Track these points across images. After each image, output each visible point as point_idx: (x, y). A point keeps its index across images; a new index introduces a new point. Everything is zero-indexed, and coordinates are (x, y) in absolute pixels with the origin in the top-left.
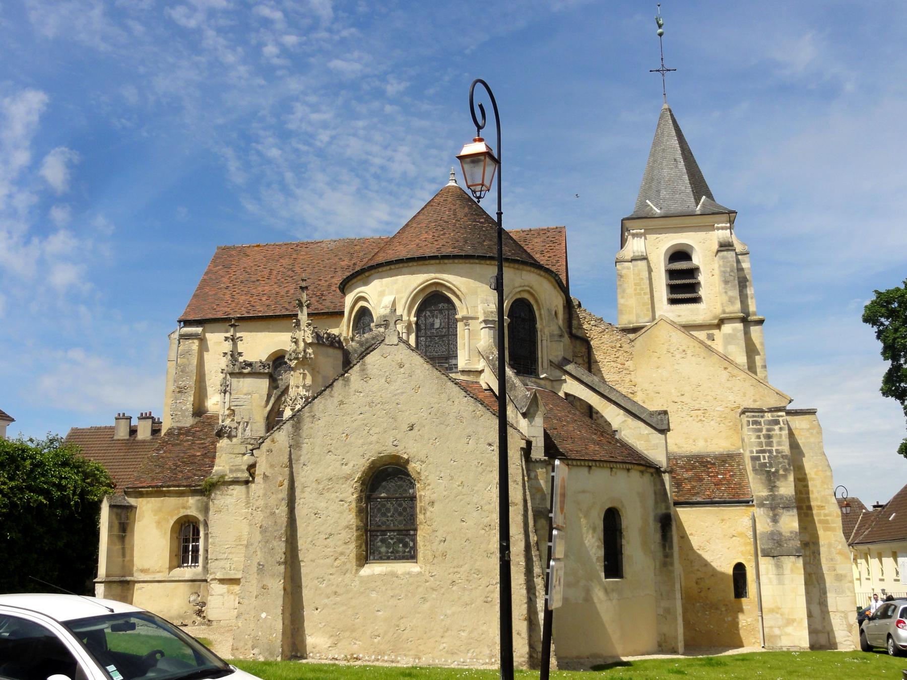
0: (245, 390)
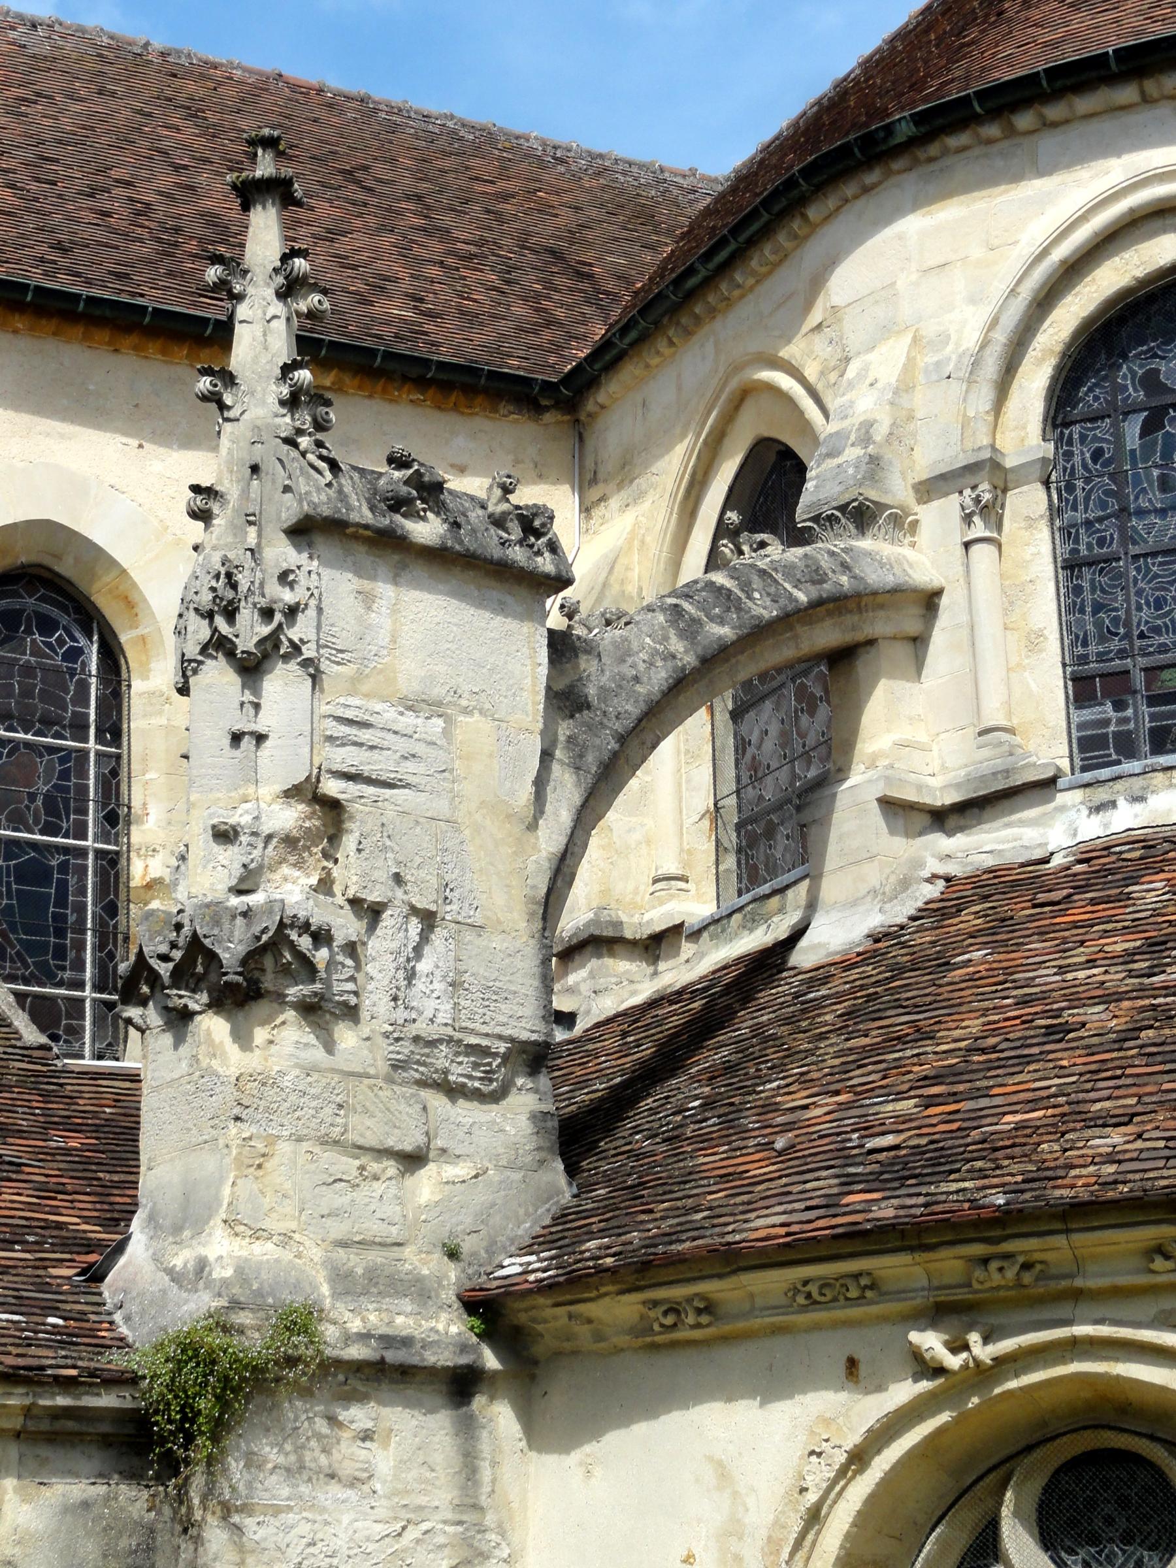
0: (410, 674)
